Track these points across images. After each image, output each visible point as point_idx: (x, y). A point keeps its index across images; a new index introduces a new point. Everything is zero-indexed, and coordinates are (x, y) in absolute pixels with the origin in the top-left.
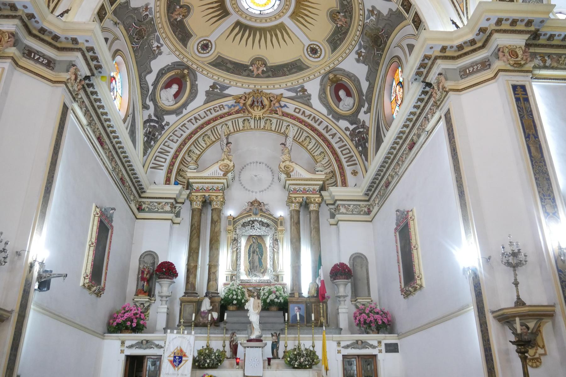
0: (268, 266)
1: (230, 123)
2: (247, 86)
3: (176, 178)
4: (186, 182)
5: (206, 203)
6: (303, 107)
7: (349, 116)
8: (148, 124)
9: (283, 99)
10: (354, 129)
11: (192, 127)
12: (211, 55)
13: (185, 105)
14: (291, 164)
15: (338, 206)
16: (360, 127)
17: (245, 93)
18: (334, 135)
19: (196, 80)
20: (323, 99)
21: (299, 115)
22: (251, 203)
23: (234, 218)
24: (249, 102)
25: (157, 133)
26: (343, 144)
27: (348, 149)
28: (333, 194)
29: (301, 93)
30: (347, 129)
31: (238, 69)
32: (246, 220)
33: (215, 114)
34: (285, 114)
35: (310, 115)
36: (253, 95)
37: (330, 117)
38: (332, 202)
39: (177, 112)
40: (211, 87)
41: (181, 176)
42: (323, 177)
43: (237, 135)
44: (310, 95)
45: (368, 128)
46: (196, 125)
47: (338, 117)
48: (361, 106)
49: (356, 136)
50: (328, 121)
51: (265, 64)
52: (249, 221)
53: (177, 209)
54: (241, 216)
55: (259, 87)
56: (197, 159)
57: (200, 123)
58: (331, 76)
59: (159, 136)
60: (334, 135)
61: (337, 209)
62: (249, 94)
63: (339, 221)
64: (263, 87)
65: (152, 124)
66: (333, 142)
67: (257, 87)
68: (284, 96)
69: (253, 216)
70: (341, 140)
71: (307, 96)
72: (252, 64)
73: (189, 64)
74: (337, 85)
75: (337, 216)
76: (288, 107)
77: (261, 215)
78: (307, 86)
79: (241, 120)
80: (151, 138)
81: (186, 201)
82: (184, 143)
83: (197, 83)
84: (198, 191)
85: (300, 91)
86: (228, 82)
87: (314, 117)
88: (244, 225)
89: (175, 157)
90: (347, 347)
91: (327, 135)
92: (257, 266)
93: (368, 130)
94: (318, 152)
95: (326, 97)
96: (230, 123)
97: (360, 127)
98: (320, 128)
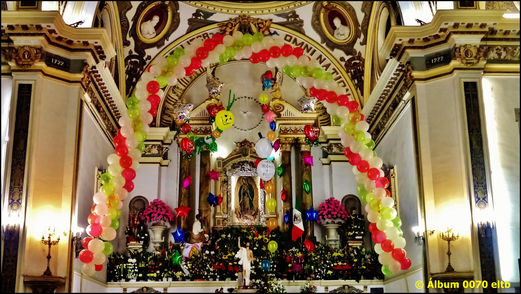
0: (260, 208)
2: (233, 12)
3: (161, 118)
4: (172, 120)
7: (345, 46)
8: (129, 61)
9: (272, 25)
10: (350, 60)
13: (167, 36)
14: (281, 103)
15: (331, 145)
16: (356, 58)
17: (231, 19)
19: (178, 9)
22: (241, 143)
23: (223, 160)
25: (138, 69)
26: (338, 75)
27: (343, 81)
28: (326, 133)
29: (292, 19)
30: (342, 59)
35: (303, 43)
36: (240, 22)
37: (324, 45)
38: (325, 141)
39: (158, 44)
40: (193, 15)
41: (167, 115)
42: (315, 116)
44: (302, 22)
45: (364, 60)
47: (333, 46)
49: (352, 67)
50: (322, 50)
52: (239, 162)
53: (164, 151)
54: (231, 158)
55: (247, 12)
56: (182, 94)
59: (141, 72)
61: (330, 147)
62: (235, 20)
63: (331, 161)
64: (250, 12)
65: (133, 60)
67: (244, 12)
68: (273, 21)
69: (243, 157)
70: (335, 71)
71: (298, 22)
75: (329, 156)
76: (278, 34)
77: (251, 156)
78: (298, 11)
81: (173, 141)
83: (178, 11)
85: (291, 17)
86: (212, 8)
87: (307, 46)
88: (234, 167)
92: (248, 209)
93: (364, 63)
95: (319, 24)
97: (356, 58)
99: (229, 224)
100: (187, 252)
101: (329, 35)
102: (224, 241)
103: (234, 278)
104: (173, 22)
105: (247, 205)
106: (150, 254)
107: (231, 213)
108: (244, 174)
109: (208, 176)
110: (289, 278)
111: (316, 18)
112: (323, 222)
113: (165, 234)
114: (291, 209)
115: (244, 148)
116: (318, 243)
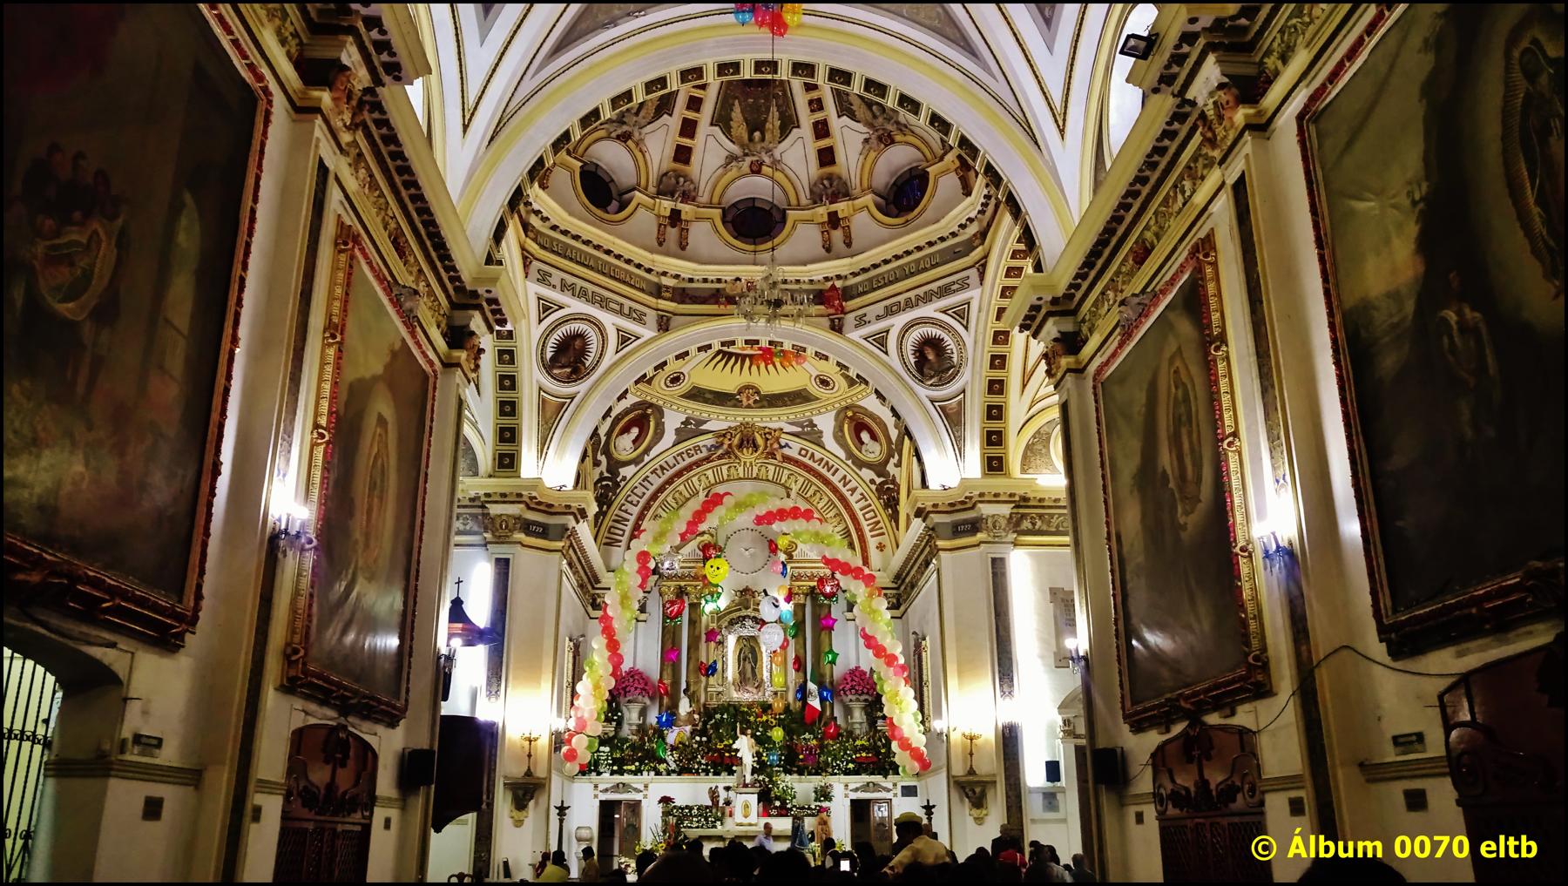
1: (709, 473)
5: (681, 593)
6: (812, 448)
10: (882, 484)
11: (657, 482)
12: (685, 387)
13: (647, 451)
18: (853, 490)
20: (839, 437)
21: (806, 460)
24: (736, 441)
30: (872, 481)
32: (734, 615)
33: (689, 461)
34: (787, 459)
39: (636, 461)
46: (664, 478)
47: (861, 464)
48: (890, 455)
50: (845, 469)
51: (758, 392)
54: (728, 611)
58: (850, 414)
60: (853, 490)
66: (852, 500)
74: (858, 424)
78: (816, 420)
79: (725, 468)
80: (604, 500)
82: (647, 507)
84: (670, 578)
88: (732, 623)
90: (856, 790)
91: (844, 490)
94: (832, 514)
96: (709, 473)
98: (835, 480)
99: (724, 699)
100: (672, 737)
101: (856, 452)
102: (720, 722)
104: (655, 432)
106: (627, 740)
107: (728, 687)
108: (745, 633)
111: (839, 430)
112: (846, 699)
113: (643, 713)
114: (805, 682)
115: (746, 596)
116: (837, 727)
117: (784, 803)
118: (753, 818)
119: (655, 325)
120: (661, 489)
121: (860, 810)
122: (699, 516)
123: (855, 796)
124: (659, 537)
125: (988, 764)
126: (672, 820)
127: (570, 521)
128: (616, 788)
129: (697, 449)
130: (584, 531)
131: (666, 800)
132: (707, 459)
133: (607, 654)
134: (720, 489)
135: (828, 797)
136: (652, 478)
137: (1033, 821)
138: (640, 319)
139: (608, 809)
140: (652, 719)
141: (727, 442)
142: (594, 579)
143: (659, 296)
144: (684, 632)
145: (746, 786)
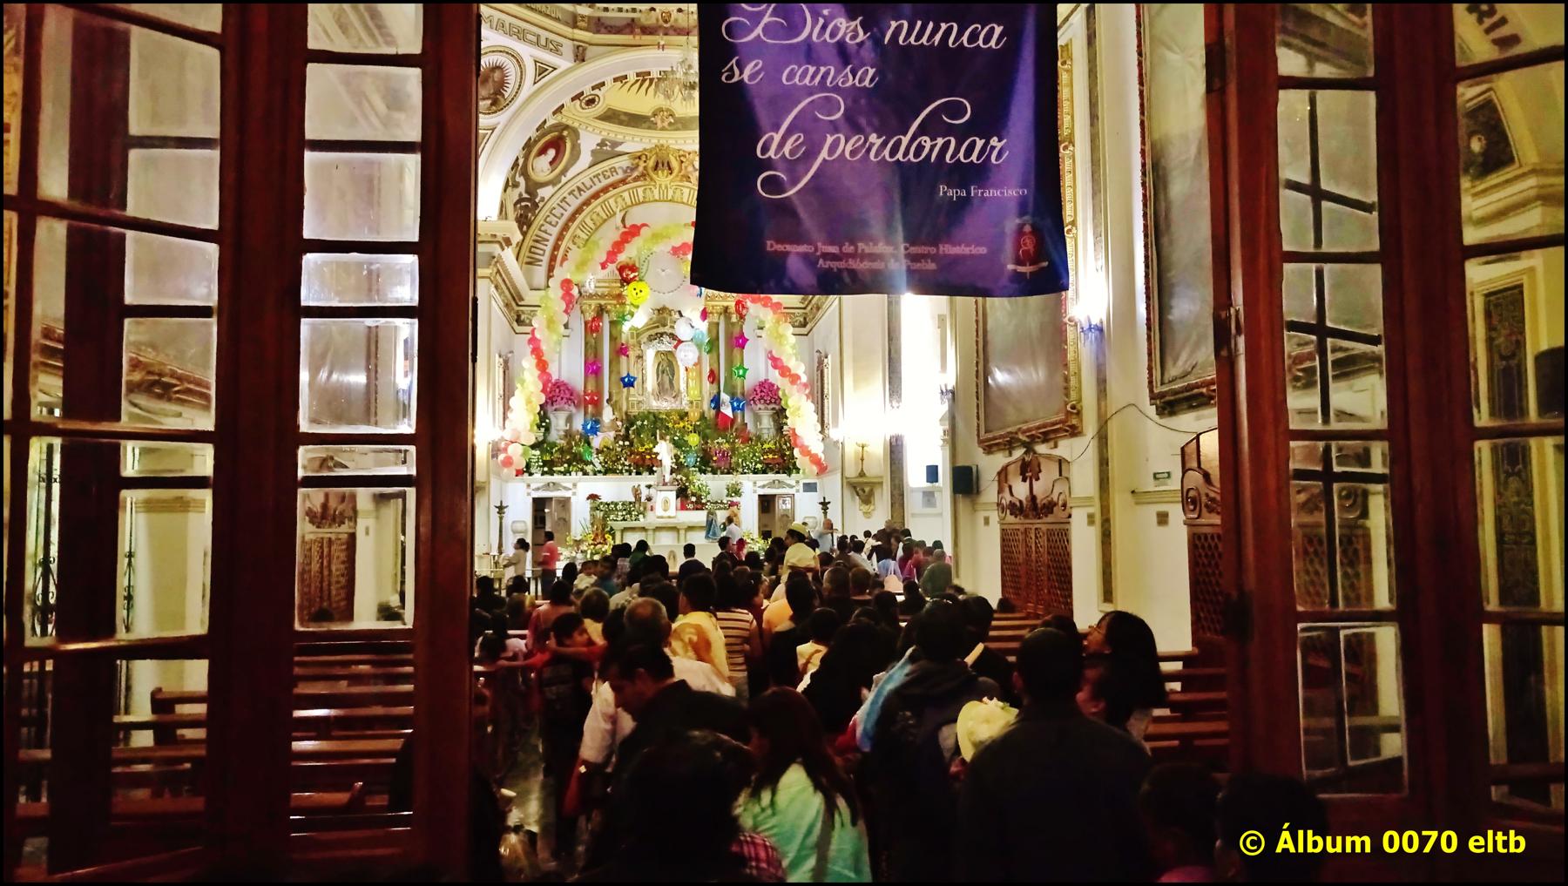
1: (626, 195)
5: (601, 311)
11: (575, 203)
12: (599, 109)
13: (564, 172)
24: (651, 163)
31: (635, 120)
33: (605, 182)
39: (552, 183)
43: (635, 209)
57: (585, 195)
62: (651, 150)
72: (655, 115)
73: (570, 123)
79: (640, 190)
80: (524, 222)
82: (566, 228)
84: (591, 296)
88: (651, 339)
89: (556, 247)
96: (626, 195)
99: (644, 408)
100: (597, 441)
103: (652, 472)
105: (667, 385)
106: (554, 445)
107: (648, 397)
108: (663, 348)
109: (621, 351)
110: (714, 472)
113: (569, 419)
115: (663, 315)
117: (699, 498)
118: (672, 511)
119: (572, 56)
120: (579, 211)
121: (766, 503)
122: (618, 247)
123: (762, 492)
124: (582, 265)
125: (877, 465)
126: (600, 514)
127: (496, 249)
128: (547, 486)
129: (613, 170)
130: (508, 255)
131: (593, 497)
132: (623, 181)
133: (537, 373)
134: (635, 217)
135: (737, 493)
136: (570, 199)
137: (913, 515)
138: (556, 50)
139: (539, 505)
140: (578, 424)
141: (642, 165)
142: (516, 297)
143: (575, 26)
144: (604, 345)
145: (665, 484)
